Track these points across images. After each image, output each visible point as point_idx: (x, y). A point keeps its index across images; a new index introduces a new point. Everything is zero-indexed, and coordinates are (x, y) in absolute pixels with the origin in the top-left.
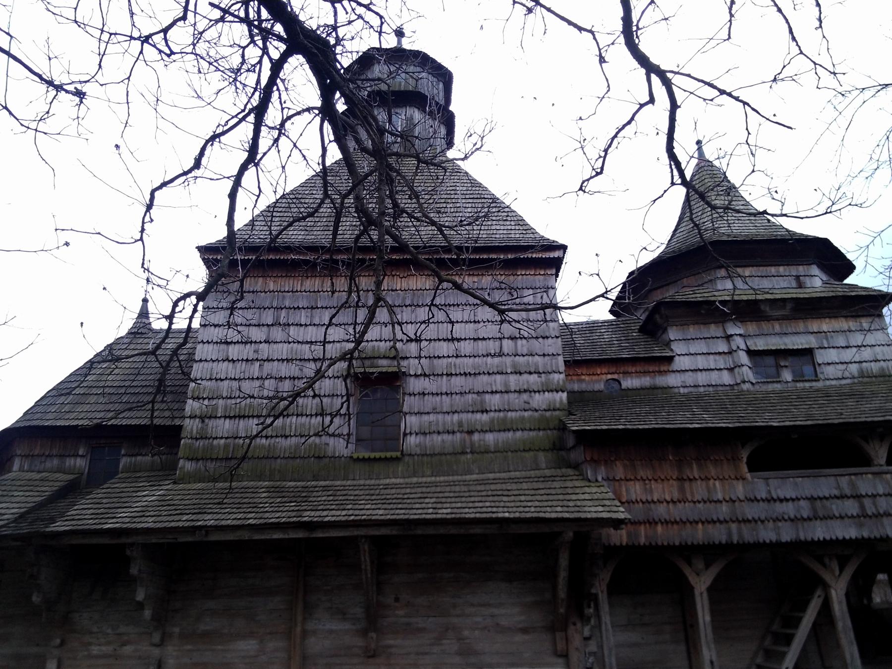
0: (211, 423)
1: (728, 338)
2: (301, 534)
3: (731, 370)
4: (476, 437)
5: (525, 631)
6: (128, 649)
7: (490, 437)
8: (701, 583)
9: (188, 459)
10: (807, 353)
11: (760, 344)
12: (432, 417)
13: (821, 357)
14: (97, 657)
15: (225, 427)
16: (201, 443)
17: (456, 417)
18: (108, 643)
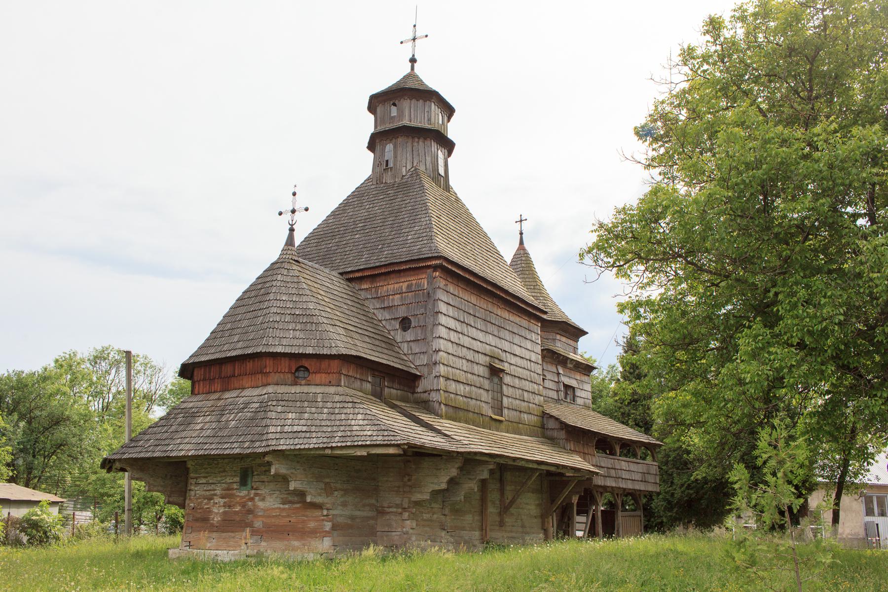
0: (448, 382)
1: (558, 374)
2: (535, 466)
3: (557, 391)
4: (522, 415)
5: (535, 517)
6: (435, 516)
7: (525, 417)
8: (575, 500)
9: (445, 405)
10: (574, 388)
11: (567, 381)
12: (510, 400)
13: (578, 393)
14: (425, 520)
15: (453, 387)
16: (446, 395)
17: (517, 402)
18: (428, 513)
